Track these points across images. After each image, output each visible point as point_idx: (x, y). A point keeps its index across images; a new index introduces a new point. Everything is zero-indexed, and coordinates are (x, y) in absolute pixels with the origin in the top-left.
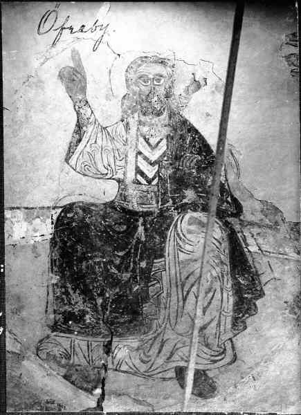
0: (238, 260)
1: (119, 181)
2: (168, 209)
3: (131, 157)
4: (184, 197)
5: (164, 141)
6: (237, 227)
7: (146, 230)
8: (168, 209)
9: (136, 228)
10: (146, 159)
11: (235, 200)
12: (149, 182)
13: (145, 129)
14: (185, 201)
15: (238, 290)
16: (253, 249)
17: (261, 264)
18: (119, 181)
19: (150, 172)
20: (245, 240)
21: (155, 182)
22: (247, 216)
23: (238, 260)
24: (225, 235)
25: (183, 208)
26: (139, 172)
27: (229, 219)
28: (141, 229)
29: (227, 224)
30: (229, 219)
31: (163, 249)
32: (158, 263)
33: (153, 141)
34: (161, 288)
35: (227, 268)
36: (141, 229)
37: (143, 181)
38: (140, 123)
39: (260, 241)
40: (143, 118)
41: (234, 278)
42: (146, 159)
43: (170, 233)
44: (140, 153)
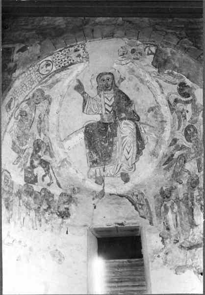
0: (139, 136)
1: (100, 114)
2: (117, 120)
3: (103, 105)
4: (122, 116)
5: (113, 98)
6: (138, 125)
7: (111, 128)
8: (117, 120)
9: (108, 128)
10: (108, 105)
11: (137, 115)
12: (110, 112)
13: (106, 95)
14: (122, 117)
15: (138, 145)
16: (143, 132)
17: (144, 136)
18: (100, 114)
19: (110, 109)
20: (141, 128)
21: (112, 113)
22: (141, 121)
23: (139, 136)
24: (134, 127)
25: (122, 119)
26: (106, 110)
27: (136, 122)
28: (109, 129)
29: (135, 123)
30: (136, 122)
31: (116, 134)
32: (115, 139)
33: (109, 99)
34: (117, 147)
35: (135, 139)
36: (109, 129)
37: (108, 113)
38: (104, 94)
39: (146, 130)
40: (105, 92)
41: (137, 142)
42: (108, 105)
43: (118, 128)
44: (106, 103)
